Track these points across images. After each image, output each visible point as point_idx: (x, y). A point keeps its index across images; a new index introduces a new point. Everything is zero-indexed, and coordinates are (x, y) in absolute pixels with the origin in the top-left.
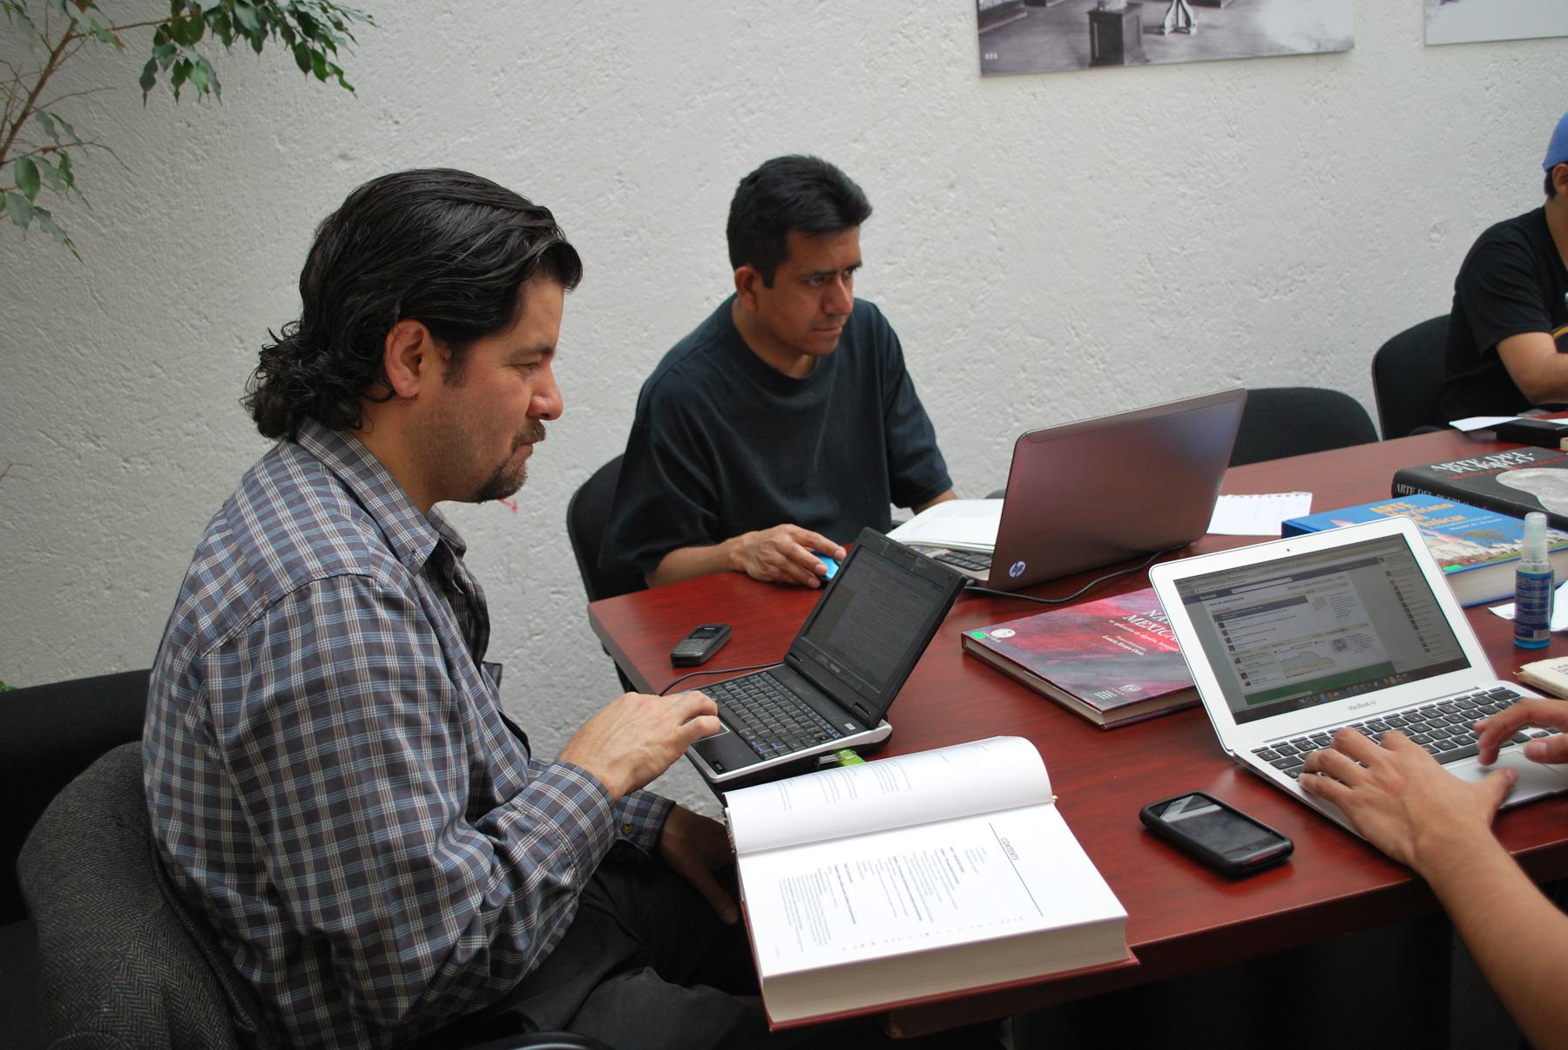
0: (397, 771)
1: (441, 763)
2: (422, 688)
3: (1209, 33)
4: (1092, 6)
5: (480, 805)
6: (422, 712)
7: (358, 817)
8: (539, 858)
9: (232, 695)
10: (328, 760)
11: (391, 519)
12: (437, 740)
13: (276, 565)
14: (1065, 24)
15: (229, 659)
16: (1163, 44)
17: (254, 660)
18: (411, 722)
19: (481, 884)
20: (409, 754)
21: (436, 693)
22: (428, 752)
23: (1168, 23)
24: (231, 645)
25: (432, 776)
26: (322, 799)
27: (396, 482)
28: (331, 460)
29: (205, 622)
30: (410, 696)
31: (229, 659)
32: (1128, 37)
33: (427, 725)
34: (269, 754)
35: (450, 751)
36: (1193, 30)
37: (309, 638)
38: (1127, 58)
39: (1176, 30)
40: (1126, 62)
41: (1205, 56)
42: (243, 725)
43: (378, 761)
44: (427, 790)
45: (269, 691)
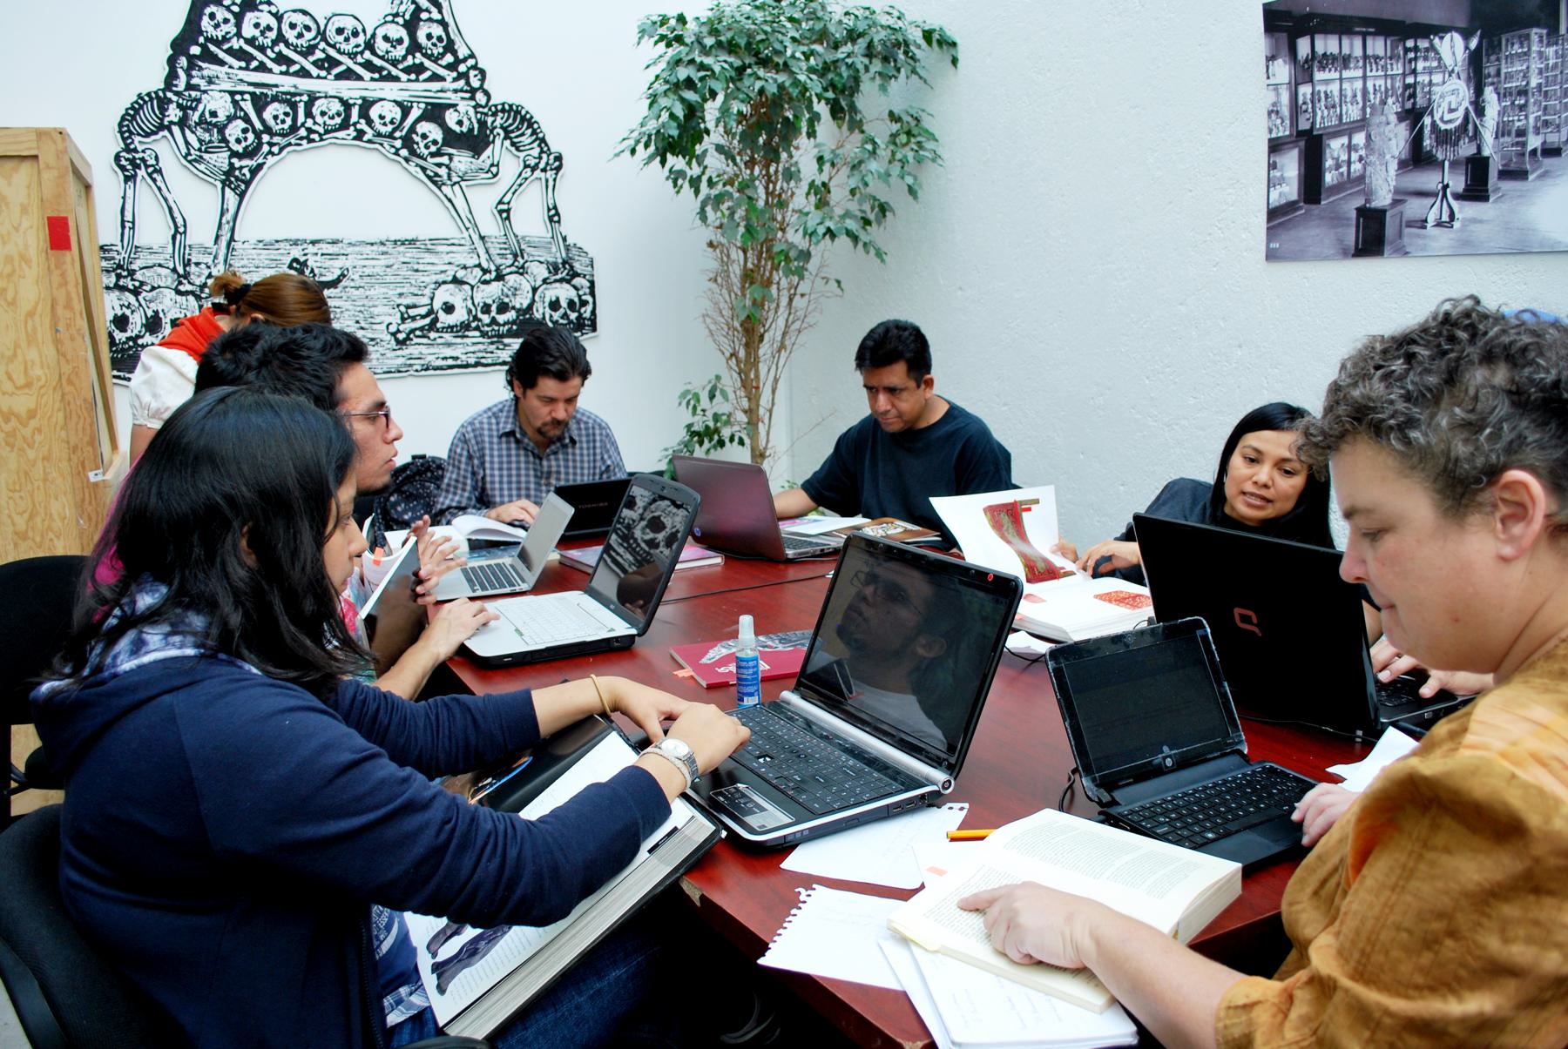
3: (1473, 227)
4: (1359, 202)
14: (1336, 219)
16: (1425, 237)
23: (1432, 218)
32: (1390, 231)
36: (1457, 224)
38: (1387, 250)
39: (1439, 224)
40: (1386, 253)
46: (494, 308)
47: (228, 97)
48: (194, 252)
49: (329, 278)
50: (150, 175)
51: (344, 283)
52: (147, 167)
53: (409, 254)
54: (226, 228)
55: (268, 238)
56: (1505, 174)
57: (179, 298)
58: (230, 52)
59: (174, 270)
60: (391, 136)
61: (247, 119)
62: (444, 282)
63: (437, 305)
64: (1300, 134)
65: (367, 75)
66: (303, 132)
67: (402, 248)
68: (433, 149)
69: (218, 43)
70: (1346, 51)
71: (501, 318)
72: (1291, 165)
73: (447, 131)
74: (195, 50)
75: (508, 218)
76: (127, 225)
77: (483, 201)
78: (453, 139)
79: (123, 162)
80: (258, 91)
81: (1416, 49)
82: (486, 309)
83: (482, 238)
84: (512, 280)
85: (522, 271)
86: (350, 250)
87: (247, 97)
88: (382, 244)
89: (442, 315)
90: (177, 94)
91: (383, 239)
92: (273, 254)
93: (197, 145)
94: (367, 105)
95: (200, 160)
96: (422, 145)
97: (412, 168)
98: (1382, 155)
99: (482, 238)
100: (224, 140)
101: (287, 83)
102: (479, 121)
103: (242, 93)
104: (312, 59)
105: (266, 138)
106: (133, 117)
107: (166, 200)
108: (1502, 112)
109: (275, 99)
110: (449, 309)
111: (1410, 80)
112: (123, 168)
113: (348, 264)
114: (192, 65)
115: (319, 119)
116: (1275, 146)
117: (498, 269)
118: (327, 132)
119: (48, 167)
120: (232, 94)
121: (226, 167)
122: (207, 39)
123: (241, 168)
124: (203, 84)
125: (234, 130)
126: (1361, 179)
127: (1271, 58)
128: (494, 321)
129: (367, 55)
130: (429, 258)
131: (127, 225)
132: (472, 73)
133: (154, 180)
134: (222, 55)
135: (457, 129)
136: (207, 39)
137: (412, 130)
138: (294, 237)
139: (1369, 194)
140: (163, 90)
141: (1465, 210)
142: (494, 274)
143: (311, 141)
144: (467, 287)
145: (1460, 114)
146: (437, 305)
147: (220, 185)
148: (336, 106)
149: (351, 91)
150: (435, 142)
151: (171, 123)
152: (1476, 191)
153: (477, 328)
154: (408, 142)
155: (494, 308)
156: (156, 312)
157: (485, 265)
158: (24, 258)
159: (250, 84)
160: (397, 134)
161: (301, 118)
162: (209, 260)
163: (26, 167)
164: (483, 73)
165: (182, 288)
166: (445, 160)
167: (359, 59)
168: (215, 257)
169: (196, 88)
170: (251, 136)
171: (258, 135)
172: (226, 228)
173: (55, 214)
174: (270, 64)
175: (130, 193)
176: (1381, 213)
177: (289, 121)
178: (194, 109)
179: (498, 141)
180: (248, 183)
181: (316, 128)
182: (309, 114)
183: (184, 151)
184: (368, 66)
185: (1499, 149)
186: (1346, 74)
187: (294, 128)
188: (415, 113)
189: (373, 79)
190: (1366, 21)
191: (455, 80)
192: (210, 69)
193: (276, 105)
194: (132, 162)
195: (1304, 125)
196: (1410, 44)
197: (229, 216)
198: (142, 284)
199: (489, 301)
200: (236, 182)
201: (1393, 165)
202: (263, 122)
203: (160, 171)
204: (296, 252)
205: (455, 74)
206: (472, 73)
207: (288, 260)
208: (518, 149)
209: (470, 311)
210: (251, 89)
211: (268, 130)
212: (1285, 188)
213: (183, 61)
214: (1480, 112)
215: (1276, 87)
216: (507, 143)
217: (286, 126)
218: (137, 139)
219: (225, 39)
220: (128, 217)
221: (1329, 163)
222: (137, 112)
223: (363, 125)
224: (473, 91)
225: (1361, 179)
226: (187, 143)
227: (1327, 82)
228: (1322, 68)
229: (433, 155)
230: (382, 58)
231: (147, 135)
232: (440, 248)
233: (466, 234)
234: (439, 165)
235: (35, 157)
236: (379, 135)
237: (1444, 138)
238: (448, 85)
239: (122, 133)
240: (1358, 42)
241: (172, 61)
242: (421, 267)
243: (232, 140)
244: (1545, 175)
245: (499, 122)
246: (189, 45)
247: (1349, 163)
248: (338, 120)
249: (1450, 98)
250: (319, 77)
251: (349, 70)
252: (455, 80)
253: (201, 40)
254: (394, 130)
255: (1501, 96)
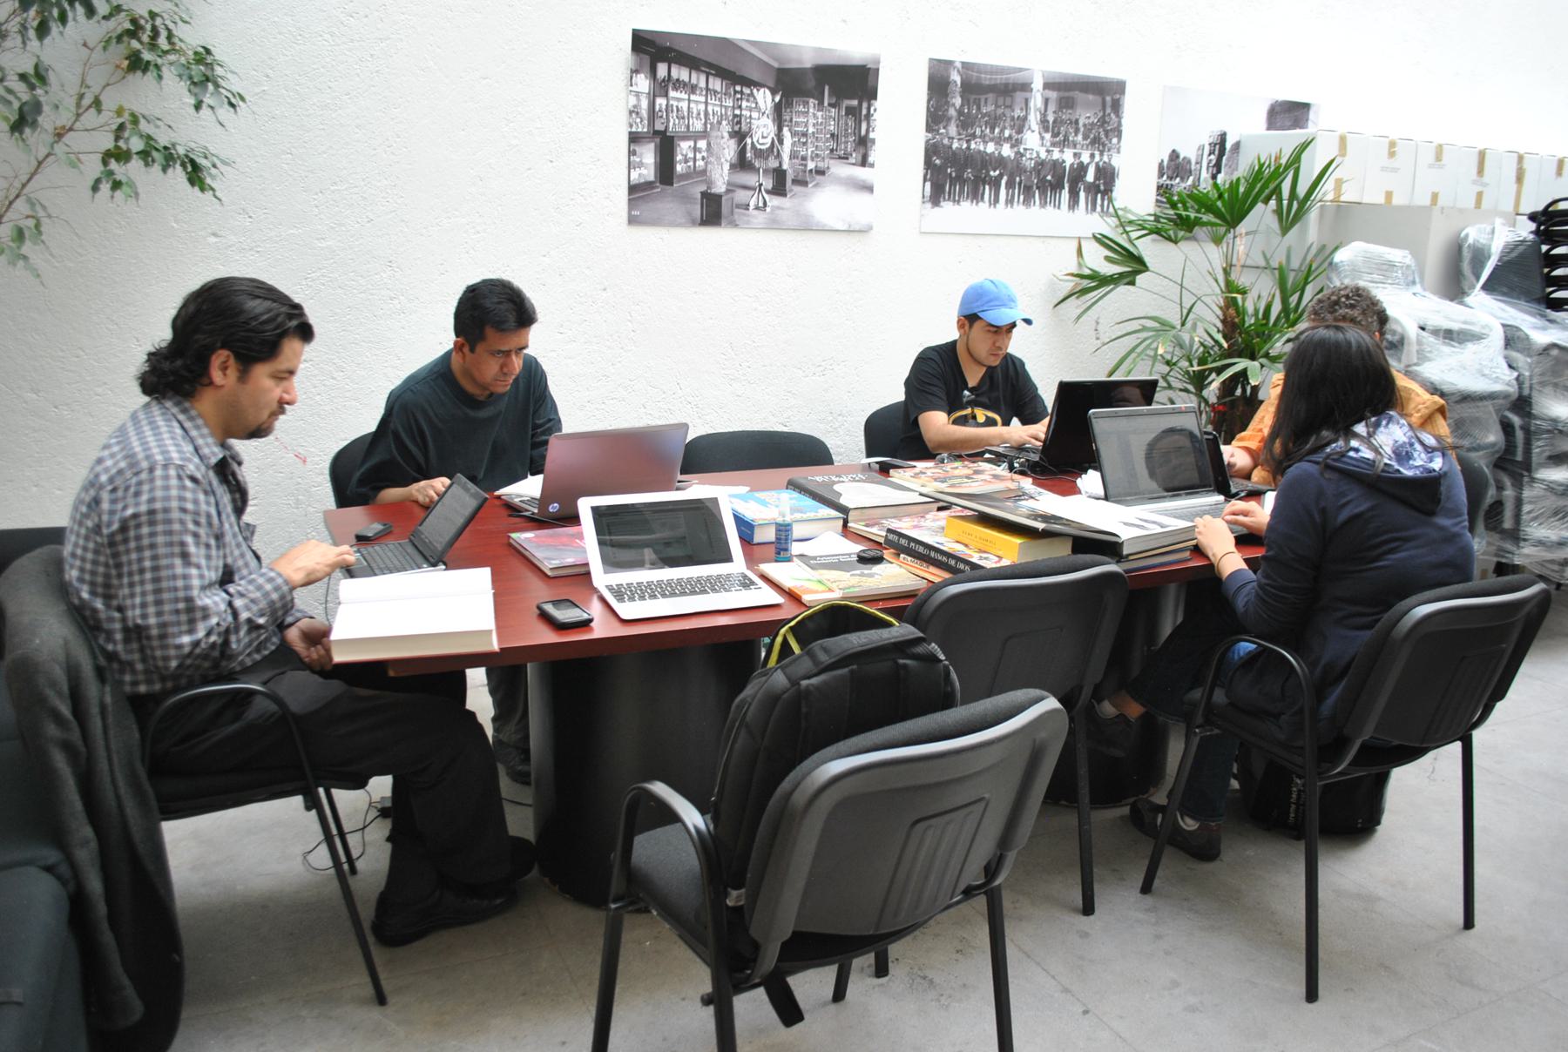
0: (185, 556)
1: (208, 557)
2: (203, 520)
4: (703, 188)
5: (227, 577)
6: (202, 531)
7: (164, 573)
8: (248, 609)
9: (112, 512)
10: (152, 546)
11: (200, 442)
12: (208, 546)
13: (141, 456)
14: (685, 198)
15: (113, 496)
17: (124, 498)
18: (196, 535)
19: (218, 614)
20: (192, 549)
21: (210, 524)
22: (203, 551)
24: (114, 490)
25: (203, 562)
26: (147, 564)
27: (207, 425)
28: (175, 410)
29: (104, 478)
30: (197, 523)
31: (113, 496)
32: (725, 209)
33: (204, 538)
34: (126, 541)
35: (214, 552)
37: (152, 490)
38: (724, 222)
39: (757, 208)
41: (774, 225)
42: (115, 526)
43: (177, 550)
44: (198, 567)
45: (130, 512)
56: (796, 182)
64: (656, 133)
70: (694, 81)
72: (648, 155)
81: (742, 93)
98: (719, 158)
108: (794, 144)
111: (737, 112)
116: (634, 138)
126: (704, 172)
127: (635, 71)
139: (710, 183)
141: (773, 201)
145: (769, 141)
152: (779, 189)
176: (718, 198)
185: (792, 165)
186: (693, 97)
190: (710, 65)
195: (659, 127)
196: (738, 88)
201: (727, 167)
212: (644, 171)
214: (781, 142)
215: (638, 94)
221: (679, 157)
225: (704, 172)
227: (679, 100)
228: (676, 89)
237: (759, 154)
240: (703, 78)
244: (816, 185)
247: (695, 160)
249: (763, 130)
255: (794, 134)
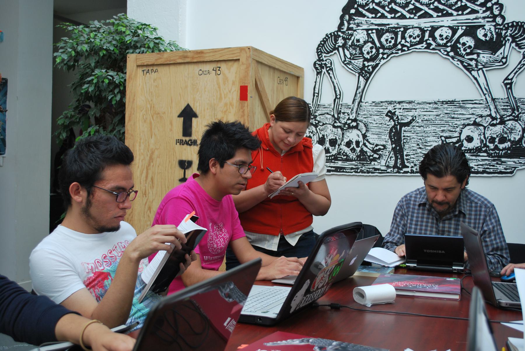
46: (497, 140)
47: (365, 32)
48: (343, 107)
49: (406, 121)
50: (327, 71)
51: (414, 124)
52: (327, 67)
53: (452, 108)
54: (358, 95)
55: (378, 100)
57: (334, 129)
58: (368, 10)
59: (333, 116)
60: (445, 45)
61: (373, 42)
62: (469, 125)
63: (463, 137)
65: (435, 14)
66: (399, 47)
67: (446, 106)
68: (468, 51)
69: (363, 6)
71: (501, 146)
73: (477, 40)
74: (353, 11)
75: (511, 88)
76: (316, 94)
77: (496, 79)
78: (480, 44)
79: (317, 66)
80: (379, 28)
82: (492, 140)
83: (493, 100)
84: (510, 124)
85: (517, 119)
86: (418, 106)
87: (374, 31)
88: (435, 103)
89: (465, 143)
90: (343, 33)
91: (436, 100)
92: (379, 108)
93: (349, 56)
94: (434, 29)
95: (350, 63)
96: (462, 49)
97: (455, 63)
99: (493, 100)
100: (362, 53)
101: (393, 23)
102: (497, 34)
103: (372, 30)
104: (407, 9)
105: (381, 51)
106: (323, 45)
107: (333, 83)
109: (388, 31)
110: (470, 139)
112: (316, 69)
113: (416, 114)
114: (351, 19)
115: (408, 40)
117: (502, 117)
118: (412, 46)
119: (243, 64)
120: (367, 30)
121: (361, 66)
122: (358, 5)
123: (369, 66)
124: (354, 27)
125: (367, 48)
128: (496, 148)
129: (436, 4)
130: (461, 111)
131: (316, 94)
132: (495, 7)
133: (329, 74)
134: (364, 12)
135: (483, 39)
136: (358, 5)
137: (458, 41)
138: (390, 100)
140: (337, 32)
142: (499, 120)
143: (403, 51)
144: (482, 128)
146: (463, 137)
147: (357, 75)
148: (417, 32)
149: (425, 23)
150: (470, 47)
151: (339, 46)
153: (485, 151)
154: (454, 48)
155: (497, 140)
156: (323, 136)
157: (494, 115)
158: (231, 104)
159: (376, 25)
160: (449, 44)
161: (399, 40)
162: (349, 111)
163: (236, 64)
164: (501, 6)
165: (336, 125)
166: (475, 56)
167: (432, 7)
168: (352, 110)
169: (351, 29)
170: (374, 50)
171: (377, 50)
172: (358, 95)
173: (243, 85)
174: (386, 14)
175: (318, 80)
177: (393, 41)
178: (350, 39)
179: (508, 45)
180: (370, 74)
181: (406, 44)
182: (403, 37)
183: (343, 59)
184: (436, 9)
187: (395, 45)
188: (460, 32)
189: (438, 16)
191: (484, 12)
192: (358, 19)
193: (387, 34)
194: (321, 65)
197: (360, 90)
198: (319, 122)
199: (495, 136)
200: (366, 74)
202: (380, 42)
203: (332, 70)
204: (390, 108)
205: (484, 9)
206: (495, 7)
207: (386, 111)
208: (520, 48)
209: (482, 141)
210: (376, 27)
211: (383, 47)
213: (347, 17)
216: (513, 45)
217: (391, 44)
218: (324, 55)
219: (367, 4)
220: (317, 91)
222: (325, 42)
223: (431, 41)
224: (494, 17)
226: (345, 55)
229: (468, 54)
230: (444, 4)
231: (328, 53)
232: (468, 106)
233: (484, 98)
234: (471, 60)
235: (239, 60)
236: (439, 45)
238: (479, 15)
239: (317, 52)
241: (342, 18)
242: (456, 116)
243: (365, 53)
245: (509, 32)
246: (351, 11)
248: (418, 39)
250: (410, 18)
251: (426, 12)
252: (484, 12)
253: (356, 6)
254: (447, 42)
